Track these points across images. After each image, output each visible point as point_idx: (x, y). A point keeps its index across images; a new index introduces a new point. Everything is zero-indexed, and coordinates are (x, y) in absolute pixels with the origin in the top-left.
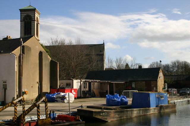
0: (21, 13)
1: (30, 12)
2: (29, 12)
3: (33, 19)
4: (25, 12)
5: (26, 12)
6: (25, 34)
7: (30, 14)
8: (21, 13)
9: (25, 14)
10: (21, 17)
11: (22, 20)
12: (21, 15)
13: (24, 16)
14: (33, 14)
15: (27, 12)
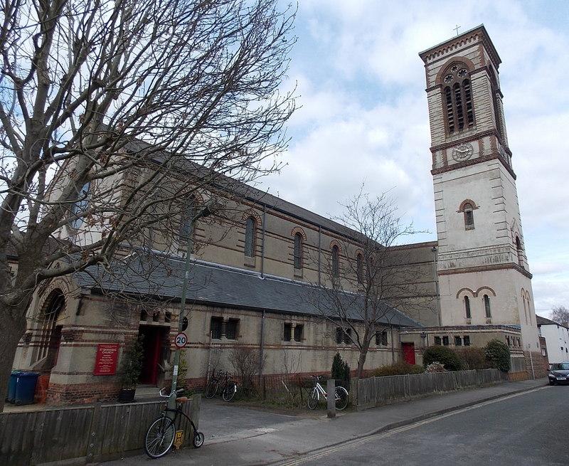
0: (429, 62)
3: (477, 67)
7: (460, 54)
8: (429, 62)
10: (427, 76)
11: (433, 85)
12: (427, 71)
13: (437, 71)
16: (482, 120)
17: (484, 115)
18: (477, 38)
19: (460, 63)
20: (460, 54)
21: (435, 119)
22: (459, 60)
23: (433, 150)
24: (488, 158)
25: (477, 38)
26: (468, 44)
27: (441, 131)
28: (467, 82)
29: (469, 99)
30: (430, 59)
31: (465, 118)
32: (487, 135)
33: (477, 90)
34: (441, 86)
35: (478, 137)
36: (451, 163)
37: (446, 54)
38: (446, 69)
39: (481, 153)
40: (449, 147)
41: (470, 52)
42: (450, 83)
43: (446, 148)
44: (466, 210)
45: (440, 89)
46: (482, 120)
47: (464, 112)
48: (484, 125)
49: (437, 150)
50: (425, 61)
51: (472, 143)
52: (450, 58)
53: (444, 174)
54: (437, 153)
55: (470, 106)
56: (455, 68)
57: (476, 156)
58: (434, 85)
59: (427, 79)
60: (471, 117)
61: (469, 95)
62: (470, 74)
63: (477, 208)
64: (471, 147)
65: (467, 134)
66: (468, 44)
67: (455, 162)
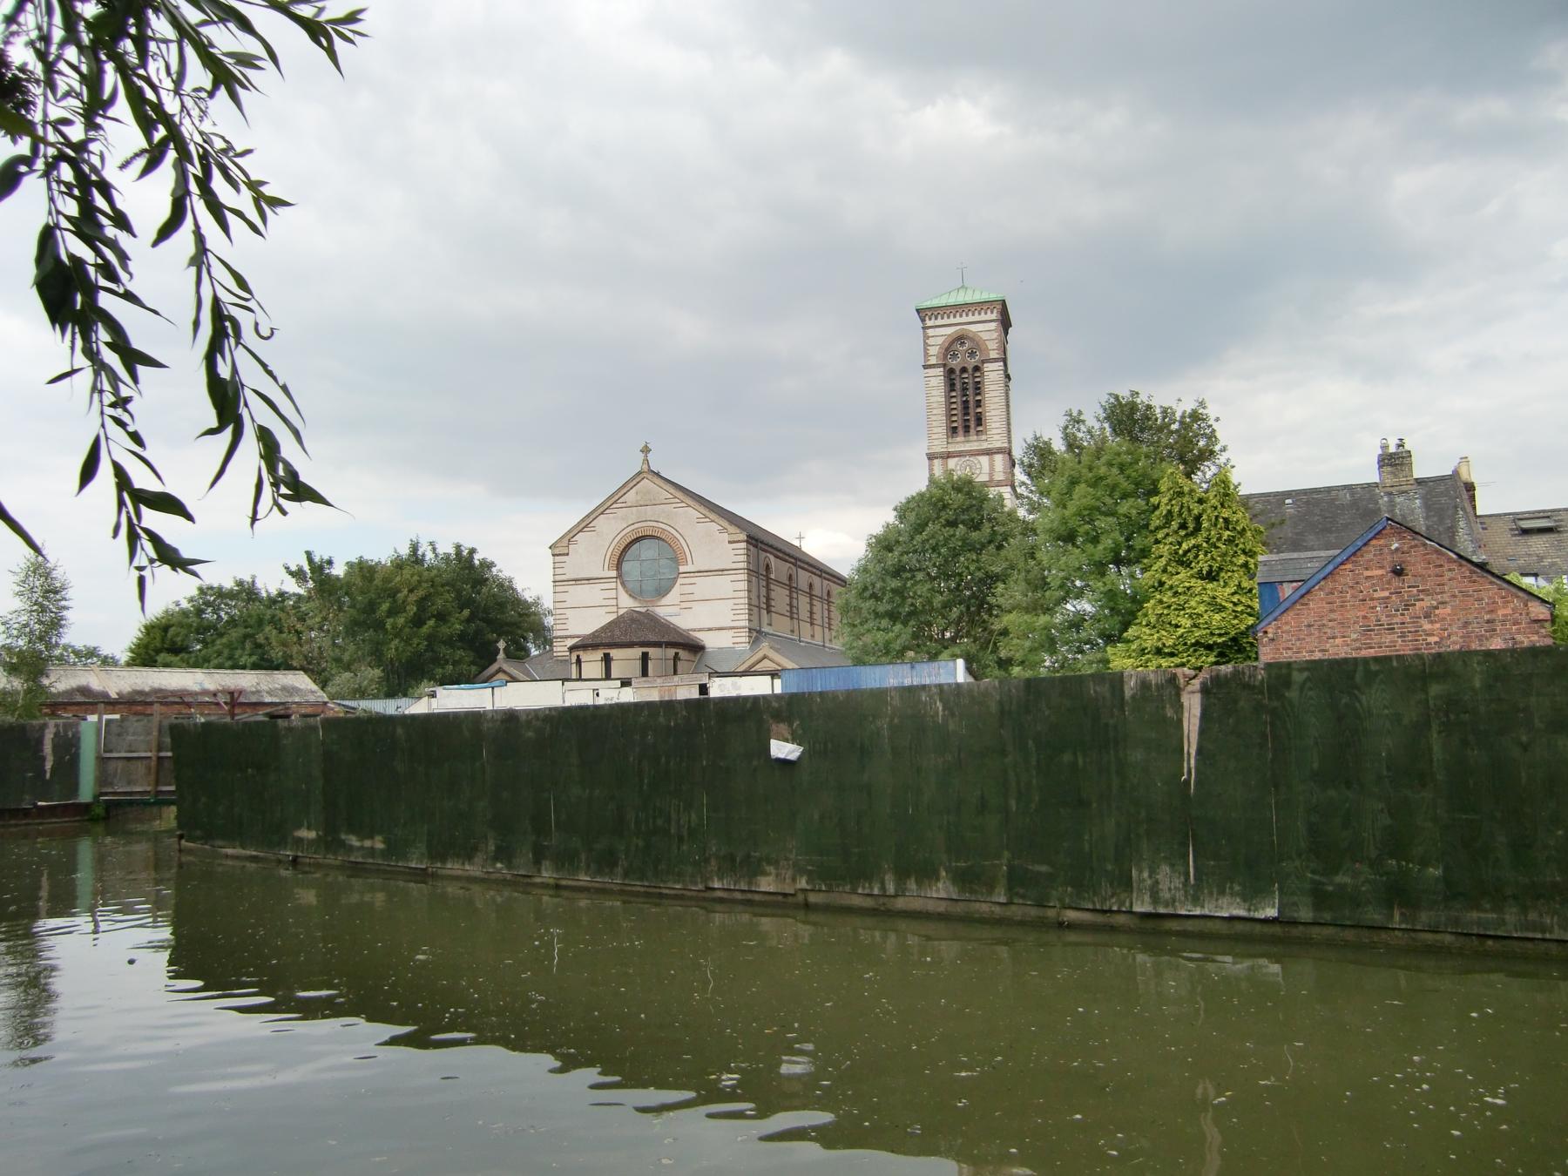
0: (929, 323)
1: (971, 318)
2: (964, 319)
3: (993, 355)
4: (946, 321)
5: (952, 320)
6: (954, 430)
7: (973, 328)
8: (929, 323)
9: (950, 331)
10: (926, 344)
11: (933, 361)
12: (926, 337)
13: (940, 341)
14: (993, 325)
15: (958, 320)
17: (998, 425)
18: (995, 311)
19: (972, 340)
20: (973, 328)
21: (935, 412)
22: (971, 335)
23: (931, 457)
25: (995, 311)
26: (983, 317)
27: (941, 429)
28: (977, 369)
29: (979, 394)
30: (930, 319)
31: (972, 418)
32: (998, 453)
33: (992, 387)
34: (944, 366)
35: (989, 452)
37: (952, 320)
38: (952, 343)
39: (991, 475)
40: (954, 457)
41: (985, 329)
42: (955, 363)
43: (948, 457)
45: (942, 369)
47: (971, 411)
48: (996, 437)
49: (936, 458)
50: (923, 320)
51: (980, 458)
52: (958, 327)
54: (936, 461)
55: (979, 404)
56: (962, 344)
58: (935, 362)
59: (926, 350)
60: (979, 420)
61: (979, 388)
62: (983, 362)
64: (979, 462)
65: (973, 444)
66: (983, 317)
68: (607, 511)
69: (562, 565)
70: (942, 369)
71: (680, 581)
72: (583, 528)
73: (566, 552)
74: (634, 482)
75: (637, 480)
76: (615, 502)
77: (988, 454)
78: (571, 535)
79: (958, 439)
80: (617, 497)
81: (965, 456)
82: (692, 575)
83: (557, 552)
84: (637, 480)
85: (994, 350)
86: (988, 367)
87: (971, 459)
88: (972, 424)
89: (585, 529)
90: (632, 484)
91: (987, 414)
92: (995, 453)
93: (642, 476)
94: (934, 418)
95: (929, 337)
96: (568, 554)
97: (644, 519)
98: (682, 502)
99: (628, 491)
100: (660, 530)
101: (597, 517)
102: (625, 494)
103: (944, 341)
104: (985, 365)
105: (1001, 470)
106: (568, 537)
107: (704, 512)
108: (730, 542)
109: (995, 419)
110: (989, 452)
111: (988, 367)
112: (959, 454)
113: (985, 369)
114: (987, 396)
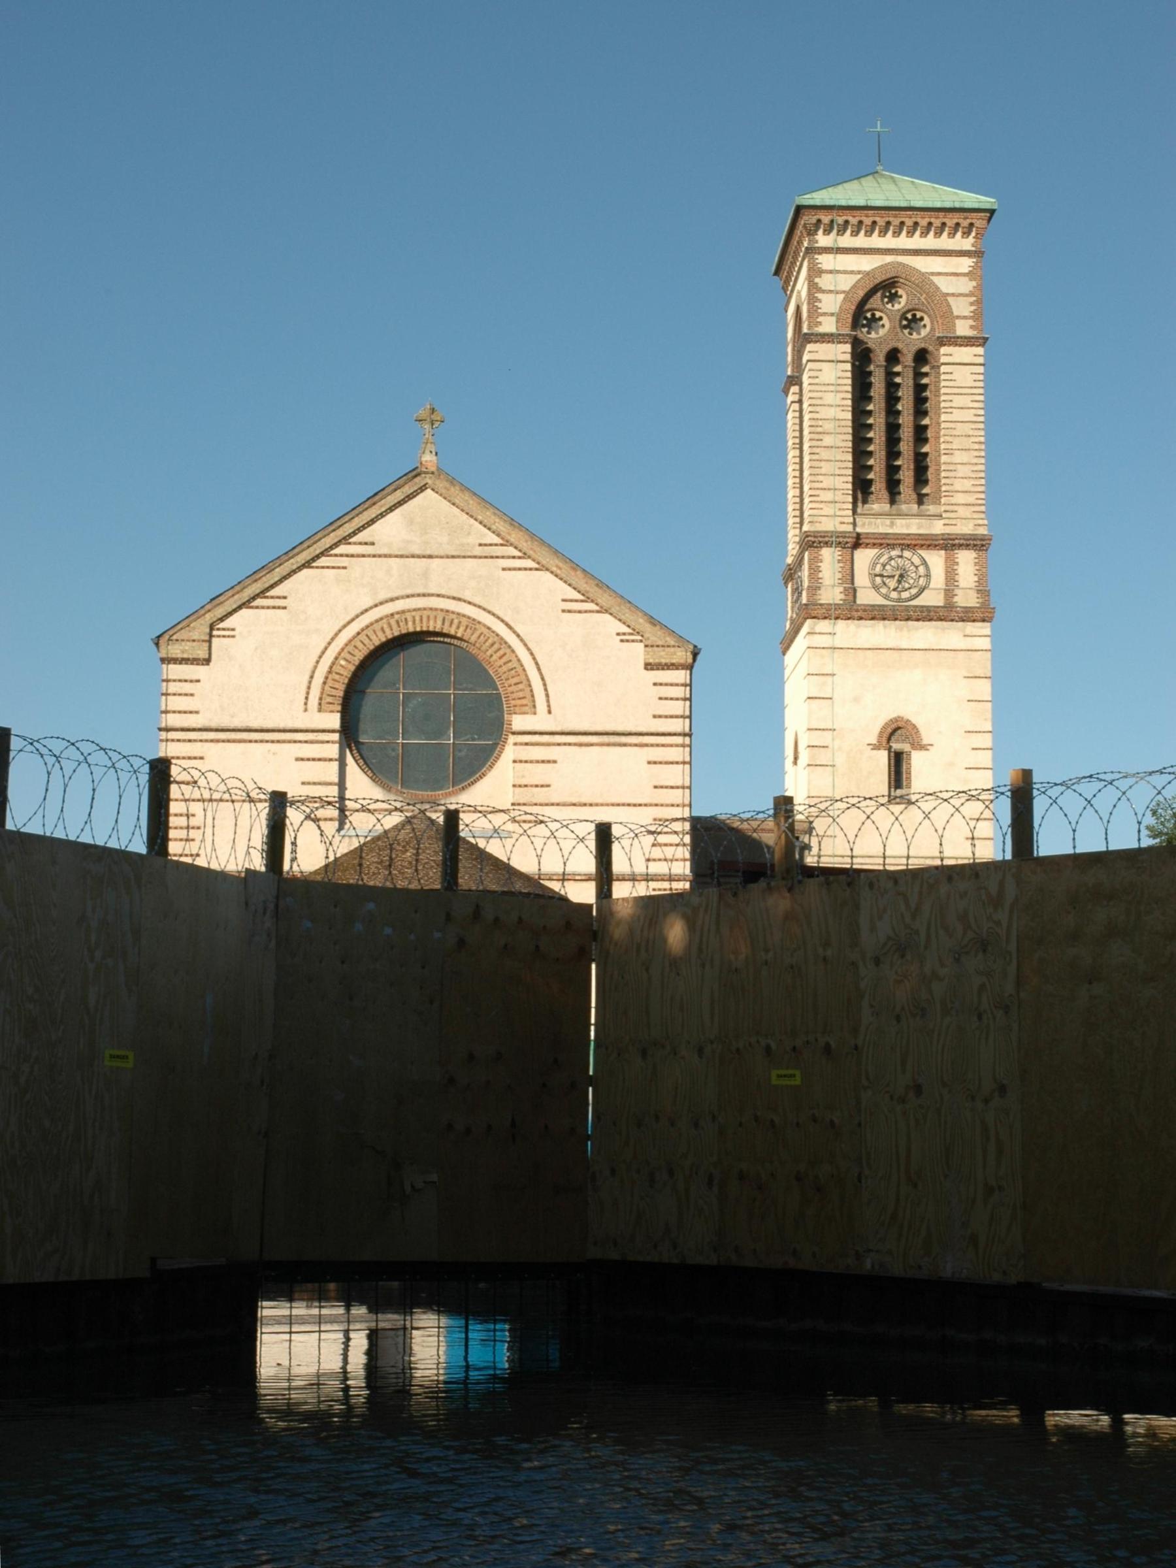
1: (917, 242)
2: (903, 241)
3: (963, 329)
4: (861, 241)
5: (876, 241)
9: (868, 264)
11: (828, 326)
13: (846, 283)
14: (966, 264)
15: (889, 241)
16: (960, 498)
17: (967, 485)
24: (967, 616)
28: (922, 357)
32: (967, 547)
33: (958, 401)
36: (867, 597)
39: (949, 593)
44: (896, 746)
46: (960, 498)
48: (962, 512)
51: (927, 555)
52: (889, 259)
53: (841, 624)
56: (893, 297)
57: (933, 598)
62: (942, 341)
63: (923, 747)
64: (924, 563)
67: (881, 601)
68: (323, 561)
69: (187, 688)
70: (848, 348)
71: (509, 752)
72: (254, 598)
73: (202, 654)
74: (399, 495)
75: (407, 490)
76: (345, 540)
77: (945, 547)
78: (220, 612)
79: (876, 507)
80: (348, 528)
81: (892, 546)
82: (546, 738)
83: (175, 650)
84: (407, 490)
85: (965, 318)
86: (947, 354)
87: (907, 554)
88: (907, 476)
89: (259, 602)
90: (392, 499)
91: (944, 459)
92: (960, 546)
93: (419, 482)
94: (825, 454)
95: (820, 272)
96: (207, 661)
97: (421, 590)
98: (525, 556)
99: (382, 515)
100: (464, 621)
101: (294, 572)
102: (372, 522)
103: (854, 287)
104: (943, 350)
105: (973, 585)
106: (209, 618)
107: (583, 586)
108: (649, 666)
109: (963, 471)
110: (949, 544)
111: (947, 354)
112: (884, 542)
113: (943, 359)
114: (943, 417)
